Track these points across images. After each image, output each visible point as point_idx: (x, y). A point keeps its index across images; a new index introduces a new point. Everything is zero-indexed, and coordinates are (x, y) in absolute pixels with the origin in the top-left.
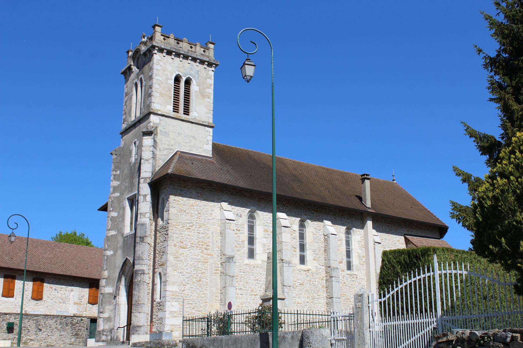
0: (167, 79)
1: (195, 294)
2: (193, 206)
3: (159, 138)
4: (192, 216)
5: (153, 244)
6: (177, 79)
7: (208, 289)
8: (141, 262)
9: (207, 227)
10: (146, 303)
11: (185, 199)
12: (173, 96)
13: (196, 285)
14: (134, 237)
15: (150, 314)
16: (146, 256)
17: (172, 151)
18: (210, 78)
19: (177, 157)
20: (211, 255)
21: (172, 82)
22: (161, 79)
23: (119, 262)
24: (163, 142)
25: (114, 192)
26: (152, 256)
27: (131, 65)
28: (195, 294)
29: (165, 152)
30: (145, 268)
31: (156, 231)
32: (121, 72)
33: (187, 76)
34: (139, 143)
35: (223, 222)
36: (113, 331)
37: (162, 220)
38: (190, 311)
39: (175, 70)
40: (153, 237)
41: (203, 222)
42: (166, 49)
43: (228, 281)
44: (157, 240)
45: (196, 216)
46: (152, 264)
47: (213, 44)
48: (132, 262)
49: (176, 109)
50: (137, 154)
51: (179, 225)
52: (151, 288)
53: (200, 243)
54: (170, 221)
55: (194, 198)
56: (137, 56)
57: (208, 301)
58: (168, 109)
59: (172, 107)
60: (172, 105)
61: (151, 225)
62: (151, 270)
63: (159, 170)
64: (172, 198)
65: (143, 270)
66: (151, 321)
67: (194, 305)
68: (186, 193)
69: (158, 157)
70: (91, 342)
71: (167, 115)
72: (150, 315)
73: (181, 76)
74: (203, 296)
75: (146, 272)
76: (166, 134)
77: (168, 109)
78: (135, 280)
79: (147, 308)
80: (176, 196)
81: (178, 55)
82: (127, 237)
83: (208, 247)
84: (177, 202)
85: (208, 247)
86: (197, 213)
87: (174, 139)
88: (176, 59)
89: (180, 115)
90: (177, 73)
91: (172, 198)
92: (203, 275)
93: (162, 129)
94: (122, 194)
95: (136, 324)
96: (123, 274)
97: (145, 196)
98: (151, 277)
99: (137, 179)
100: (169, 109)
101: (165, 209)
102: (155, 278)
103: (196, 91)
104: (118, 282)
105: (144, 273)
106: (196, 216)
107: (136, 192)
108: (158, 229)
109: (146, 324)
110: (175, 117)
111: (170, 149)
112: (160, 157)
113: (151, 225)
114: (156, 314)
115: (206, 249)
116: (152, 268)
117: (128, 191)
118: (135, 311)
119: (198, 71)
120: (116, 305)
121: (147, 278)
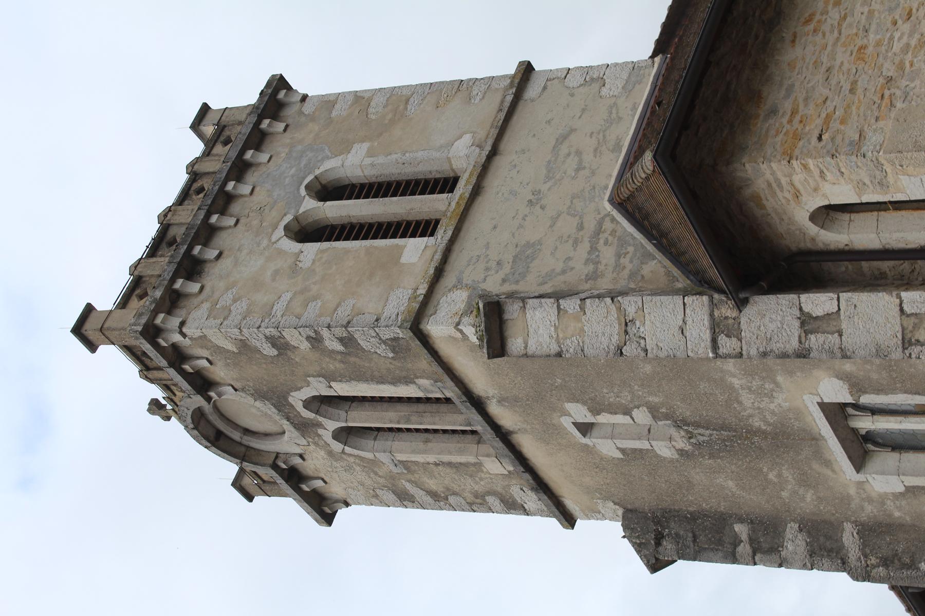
0: (294, 269)
3: (529, 285)
6: (307, 232)
17: (608, 225)
21: (311, 249)
22: (288, 296)
24: (560, 266)
29: (607, 254)
32: (325, 529)
33: (303, 192)
34: (574, 399)
39: (265, 242)
42: (173, 280)
49: (424, 228)
56: (236, 435)
71: (438, 257)
77: (414, 260)
84: (835, 125)
86: (906, 27)
87: (555, 220)
88: (222, 240)
89: (453, 204)
90: (280, 231)
93: (501, 275)
97: (808, 323)
100: (415, 252)
103: (370, 153)
110: (454, 222)
111: (599, 231)
112: (626, 272)
117: (816, 466)
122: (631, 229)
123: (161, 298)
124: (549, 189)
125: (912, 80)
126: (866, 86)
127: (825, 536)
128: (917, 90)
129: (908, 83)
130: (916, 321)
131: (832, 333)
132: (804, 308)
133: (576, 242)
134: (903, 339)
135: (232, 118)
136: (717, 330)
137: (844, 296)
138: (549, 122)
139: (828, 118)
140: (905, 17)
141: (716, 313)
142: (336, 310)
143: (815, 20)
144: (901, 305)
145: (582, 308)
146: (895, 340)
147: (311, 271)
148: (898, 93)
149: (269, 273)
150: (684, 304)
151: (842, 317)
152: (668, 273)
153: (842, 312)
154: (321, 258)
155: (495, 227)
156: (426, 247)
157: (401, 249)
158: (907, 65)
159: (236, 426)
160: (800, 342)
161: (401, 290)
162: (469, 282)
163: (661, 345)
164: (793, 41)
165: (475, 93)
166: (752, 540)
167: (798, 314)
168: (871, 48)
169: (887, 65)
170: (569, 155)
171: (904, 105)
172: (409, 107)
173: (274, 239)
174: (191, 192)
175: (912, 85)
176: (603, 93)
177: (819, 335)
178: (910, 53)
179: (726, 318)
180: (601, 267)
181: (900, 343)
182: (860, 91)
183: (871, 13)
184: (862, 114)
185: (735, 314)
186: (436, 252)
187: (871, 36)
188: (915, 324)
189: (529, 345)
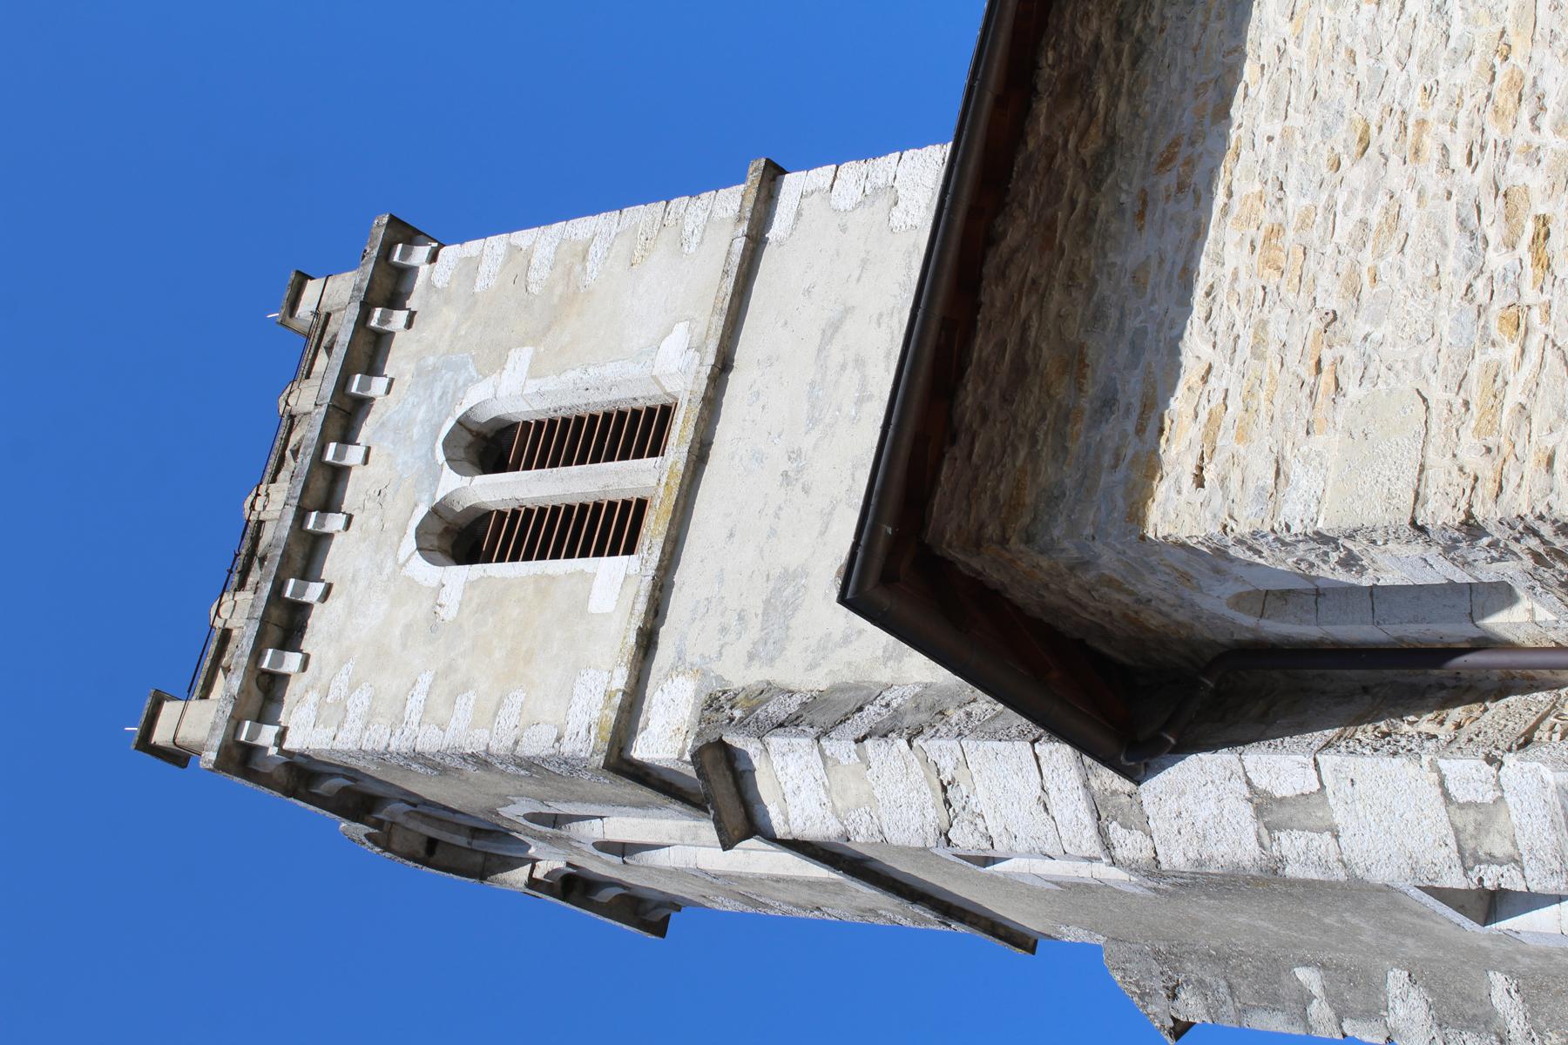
0: (434, 622)
2: (1276, 231)
4: (1394, 218)
11: (1196, 347)
18: (471, 267)
25: (1484, 1021)
27: (533, 883)
37: (1503, 595)
39: (389, 566)
41: (1464, 75)
42: (257, 654)
45: (1396, 176)
47: (303, 278)
51: (1495, 375)
54: (1442, 513)
55: (1199, 232)
56: (462, 841)
59: (606, 561)
64: (1176, 512)
68: (1136, 349)
73: (435, 511)
80: (1150, 466)
81: (308, 552)
86: (1356, 174)
88: (334, 564)
90: (410, 543)
91: (1176, 512)
94: (1485, 961)
101: (1331, 572)
103: (534, 373)
106: (1396, 176)
119: (419, 372)
123: (241, 691)
124: (815, 447)
125: (1377, 324)
126: (1284, 337)
127: (1459, 994)
128: (1386, 350)
129: (1368, 329)
130: (1480, 817)
131: (1320, 831)
132: (1255, 782)
134: (1460, 850)
135: (337, 300)
136: (1104, 815)
137: (1328, 760)
138: (808, 291)
139: (1213, 423)
140: (1356, 148)
141: (1095, 783)
142: (496, 714)
143: (1180, 159)
144: (1442, 783)
145: (863, 758)
146: (1444, 851)
148: (1351, 356)
149: (397, 631)
150: (1037, 758)
151: (1332, 801)
153: (1329, 791)
154: (471, 599)
155: (731, 535)
156: (627, 576)
157: (588, 578)
158: (1366, 279)
159: (458, 828)
160: (1262, 845)
161: (592, 672)
162: (697, 659)
163: (1013, 830)
164: (1141, 215)
165: (689, 229)
166: (1334, 998)
167: (1246, 791)
168: (1290, 234)
169: (1326, 280)
170: (843, 367)
171: (1362, 392)
172: (589, 265)
174: (288, 453)
175: (1377, 335)
176: (895, 222)
177: (1296, 833)
178: (1369, 245)
179: (1114, 793)
181: (1455, 856)
182: (1272, 349)
184: (1277, 416)
185: (1128, 786)
186: (637, 595)
187: (1290, 201)
188: (1478, 825)
189: (791, 816)
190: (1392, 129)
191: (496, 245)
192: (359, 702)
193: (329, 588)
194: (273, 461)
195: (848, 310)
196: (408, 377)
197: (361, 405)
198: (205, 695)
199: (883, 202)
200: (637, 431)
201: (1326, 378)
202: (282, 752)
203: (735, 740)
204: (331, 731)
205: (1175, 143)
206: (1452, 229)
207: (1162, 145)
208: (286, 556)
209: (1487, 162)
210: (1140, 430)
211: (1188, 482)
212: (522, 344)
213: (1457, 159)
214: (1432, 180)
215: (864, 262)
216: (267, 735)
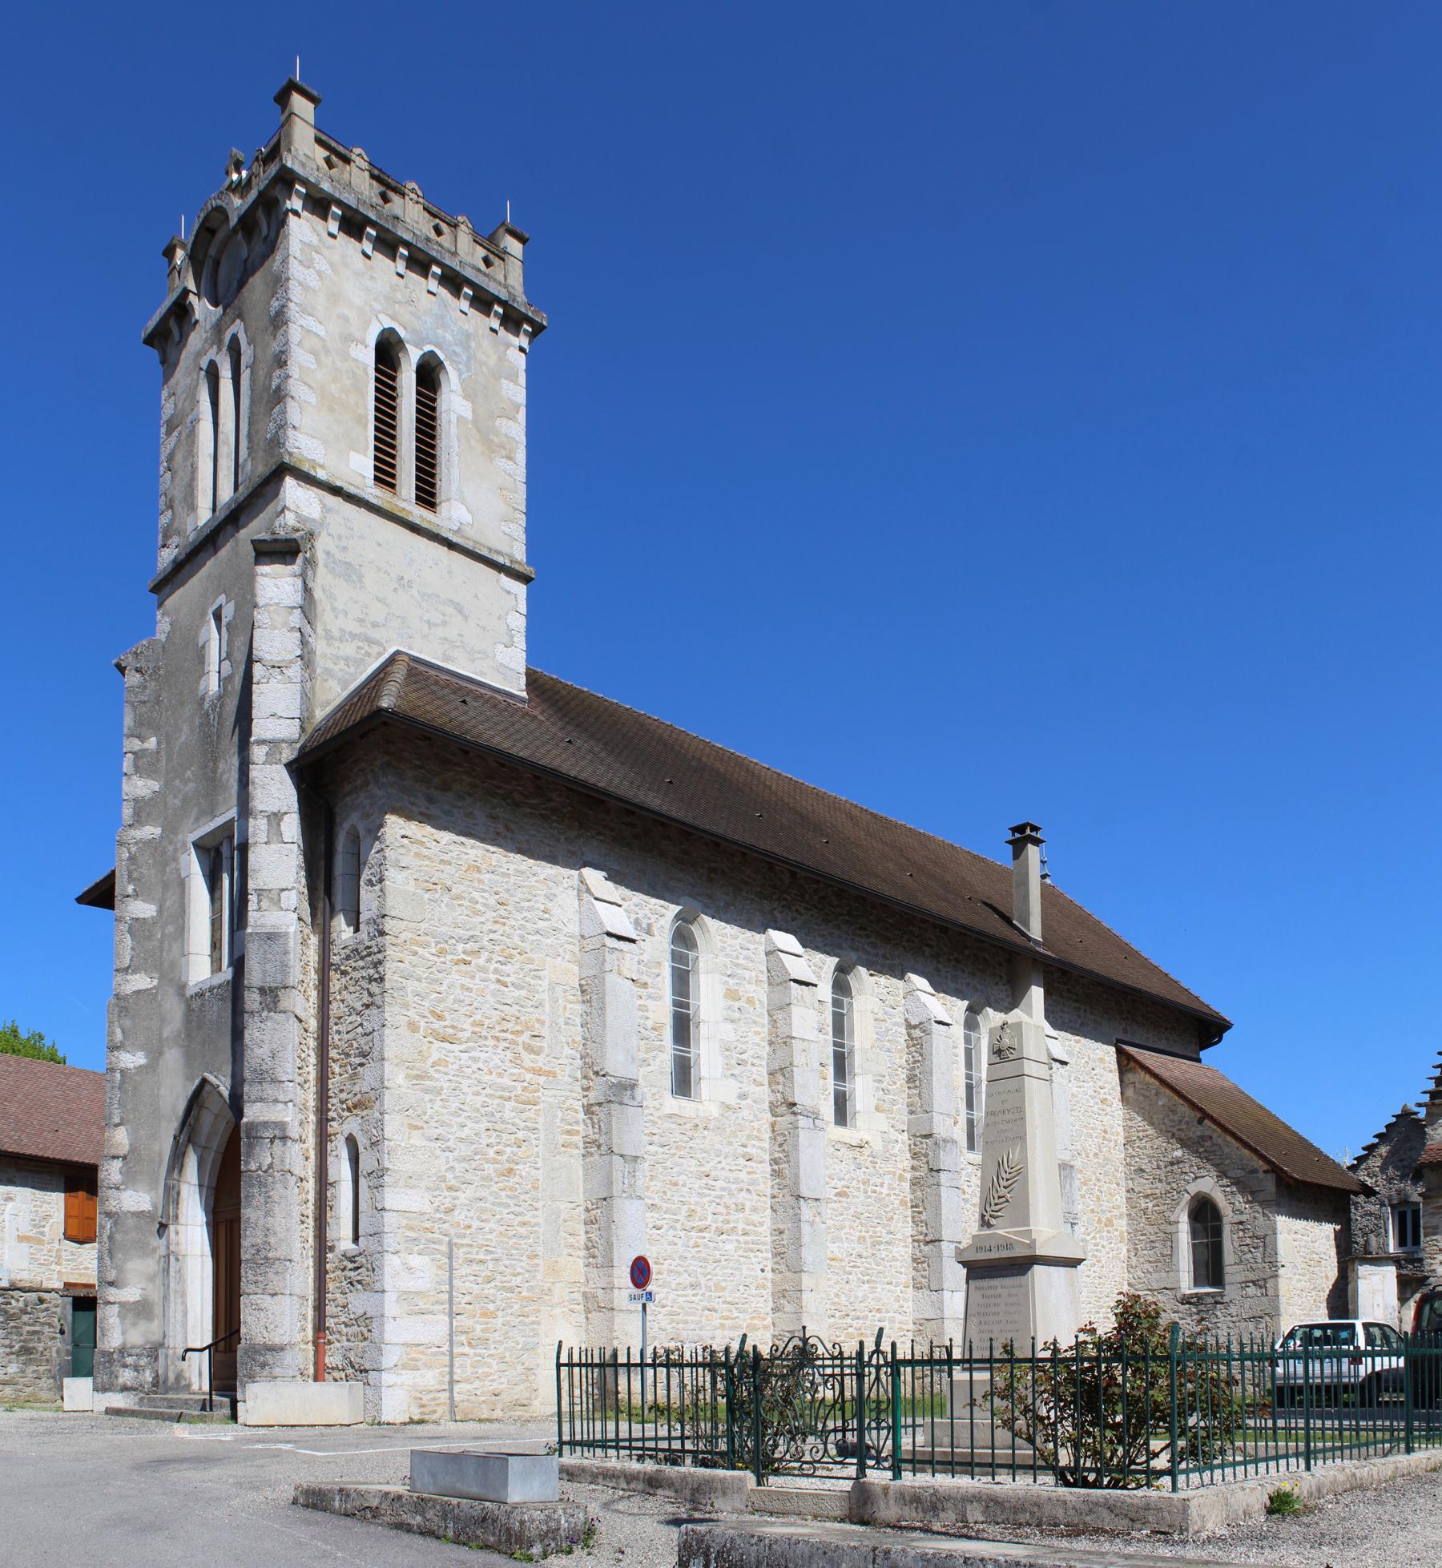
1: (492, 1225)
5: (313, 1024)
7: (539, 1205)
8: (270, 1090)
9: (531, 961)
10: (296, 1256)
12: (372, 413)
13: (495, 1188)
14: (228, 995)
15: (311, 1298)
16: (289, 1068)
19: (399, 673)
20: (549, 1073)
21: (369, 357)
23: (174, 1095)
24: (339, 605)
26: (312, 1073)
28: (492, 1225)
29: (349, 649)
30: (288, 1115)
31: (325, 968)
35: (594, 943)
36: (161, 1352)
38: (476, 1289)
39: (378, 307)
40: (314, 994)
41: (516, 939)
43: (617, 1176)
44: (334, 1006)
46: (312, 1103)
48: (226, 1093)
50: (229, 656)
52: (311, 1196)
53: (509, 1026)
57: (540, 1250)
58: (353, 465)
59: (371, 463)
60: (371, 452)
61: (304, 943)
62: (311, 1128)
63: (328, 718)
65: (281, 1126)
66: (320, 1327)
67: (491, 1265)
69: (321, 664)
70: (79, 1392)
71: (352, 490)
72: (311, 1302)
74: (522, 1230)
75: (294, 1131)
76: (350, 572)
77: (353, 465)
78: (250, 1165)
79: (301, 1277)
81: (388, 244)
82: (200, 995)
83: (536, 1043)
85: (536, 1043)
92: (520, 1152)
95: (259, 1340)
96: (189, 1140)
98: (312, 1154)
99: (235, 761)
100: (358, 469)
102: (330, 1159)
104: (170, 1170)
105: (284, 1138)
107: (233, 813)
108: (335, 959)
109: (298, 1338)
113: (304, 943)
114: (341, 1299)
115: (530, 1049)
116: (312, 1118)
118: (251, 1288)
120: (169, 1260)
121: (299, 1157)
122: (370, 670)
133: (361, 621)
147: (346, 357)
152: (328, 703)
157: (364, 453)
173: (382, 317)
180: (336, 644)
183: (508, 876)
190: (504, 913)
191: (521, 396)
192: (312, 279)
193: (369, 257)
194: (434, 210)
195: (466, 618)
196: (466, 327)
197: (456, 292)
198: (318, 141)
199: (506, 640)
200: (427, 496)
201: (432, 887)
202: (288, 210)
203: (299, 560)
204: (298, 255)
205: (512, 831)
206: (471, 933)
207: (513, 826)
208: (388, 231)
209: (490, 946)
210: (421, 814)
211: (403, 832)
212: (474, 412)
213: (492, 936)
214: (489, 926)
215: (484, 628)
216: (296, 203)
